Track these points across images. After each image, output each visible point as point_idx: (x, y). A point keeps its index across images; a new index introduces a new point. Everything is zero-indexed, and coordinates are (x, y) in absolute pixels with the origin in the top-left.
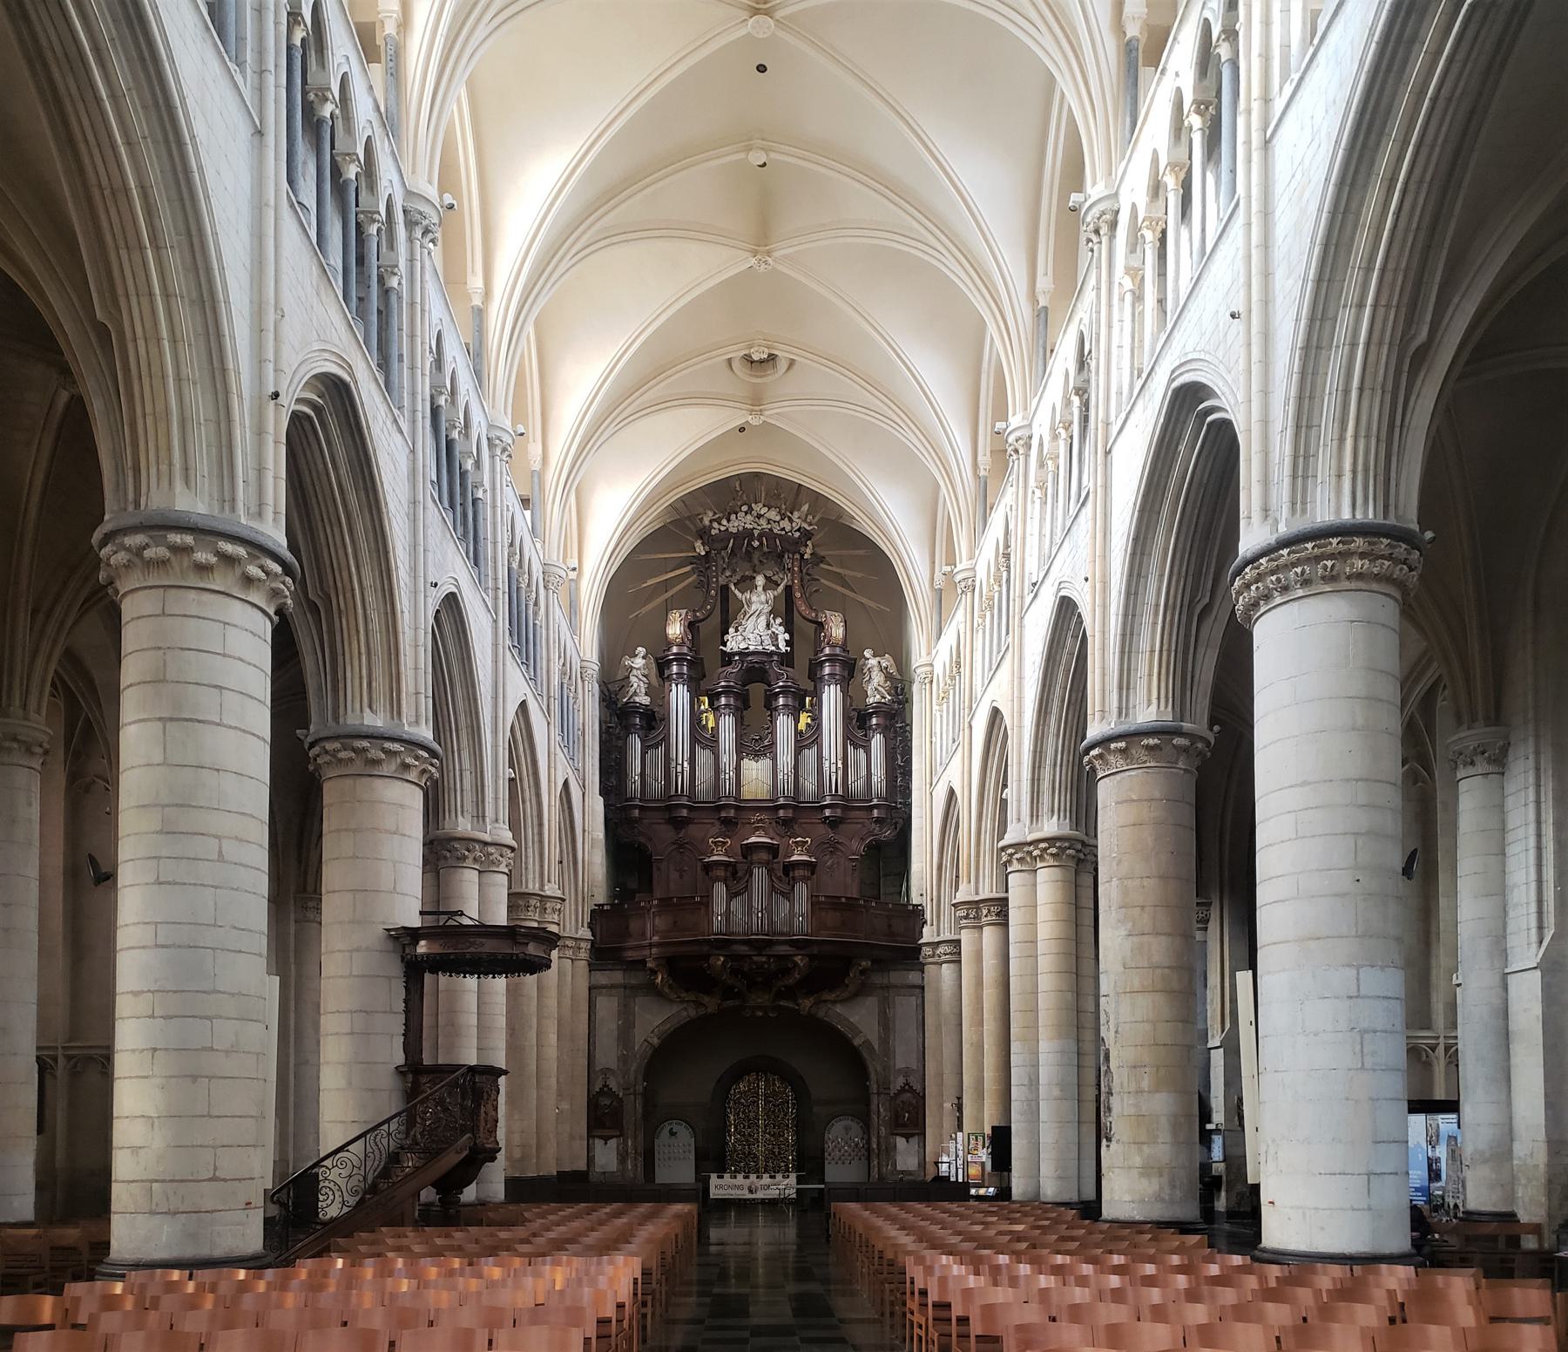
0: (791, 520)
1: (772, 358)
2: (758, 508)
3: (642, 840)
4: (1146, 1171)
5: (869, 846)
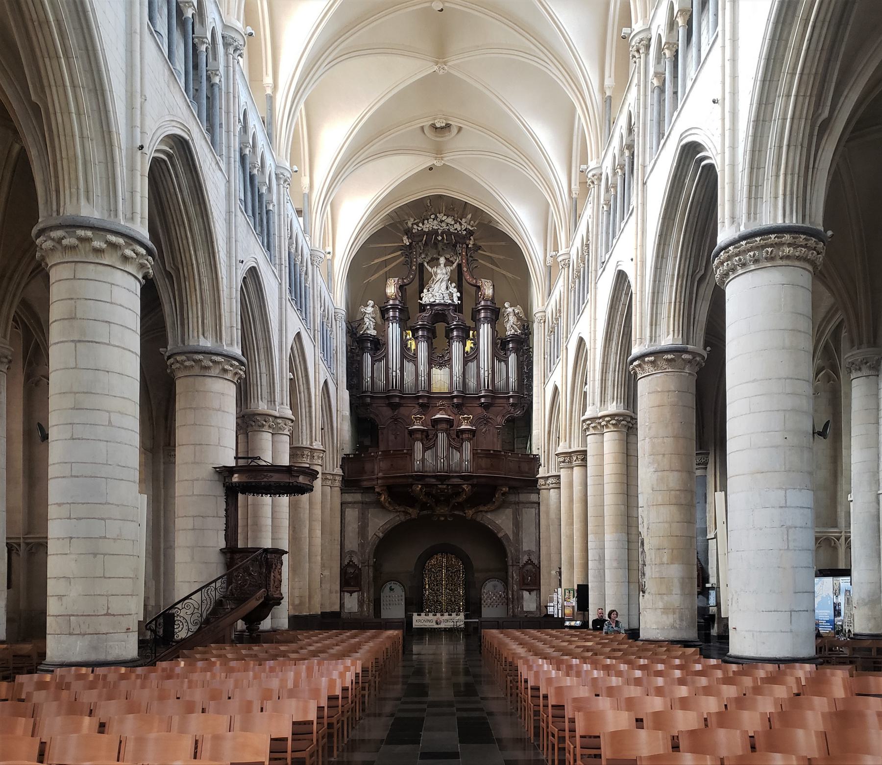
1: (448, 126)
2: (441, 216)
3: (372, 416)
5: (508, 421)
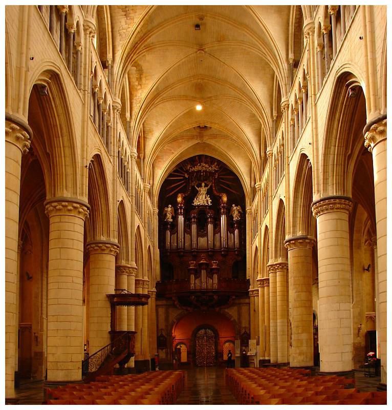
0: (212, 168)
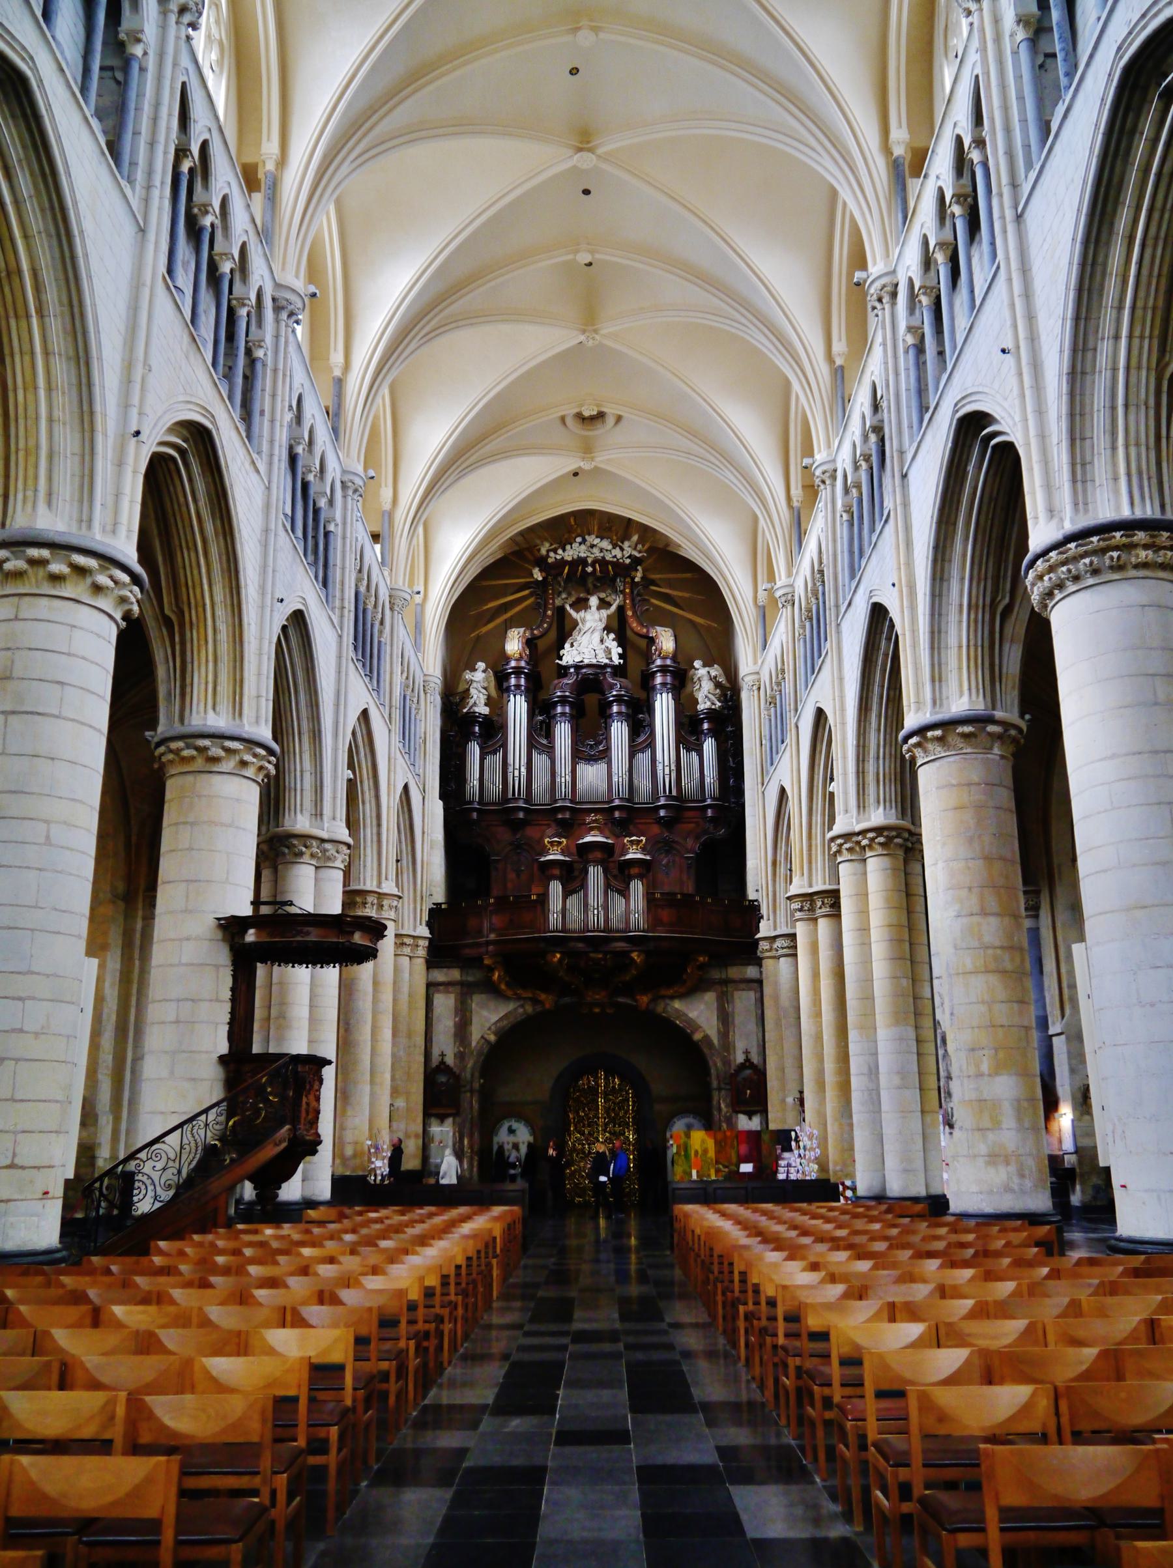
0: (622, 549)
2: (592, 539)
4: (995, 1158)
5: (704, 845)
